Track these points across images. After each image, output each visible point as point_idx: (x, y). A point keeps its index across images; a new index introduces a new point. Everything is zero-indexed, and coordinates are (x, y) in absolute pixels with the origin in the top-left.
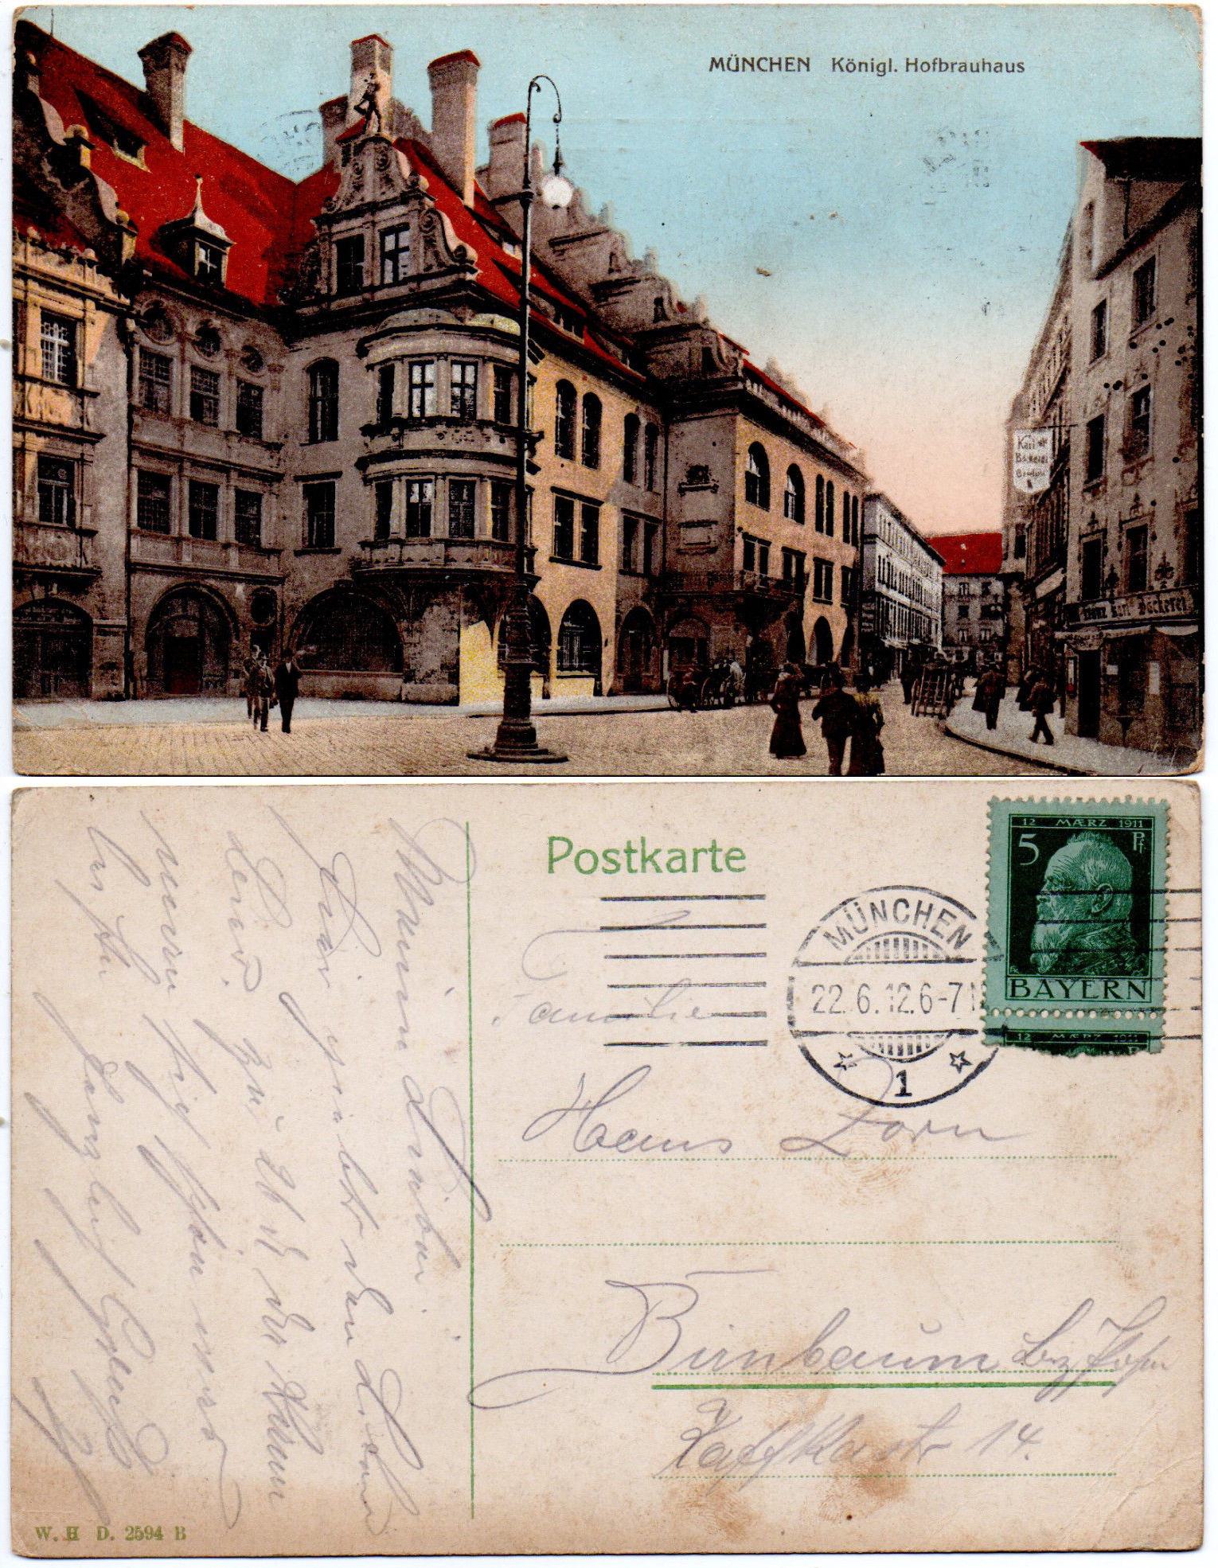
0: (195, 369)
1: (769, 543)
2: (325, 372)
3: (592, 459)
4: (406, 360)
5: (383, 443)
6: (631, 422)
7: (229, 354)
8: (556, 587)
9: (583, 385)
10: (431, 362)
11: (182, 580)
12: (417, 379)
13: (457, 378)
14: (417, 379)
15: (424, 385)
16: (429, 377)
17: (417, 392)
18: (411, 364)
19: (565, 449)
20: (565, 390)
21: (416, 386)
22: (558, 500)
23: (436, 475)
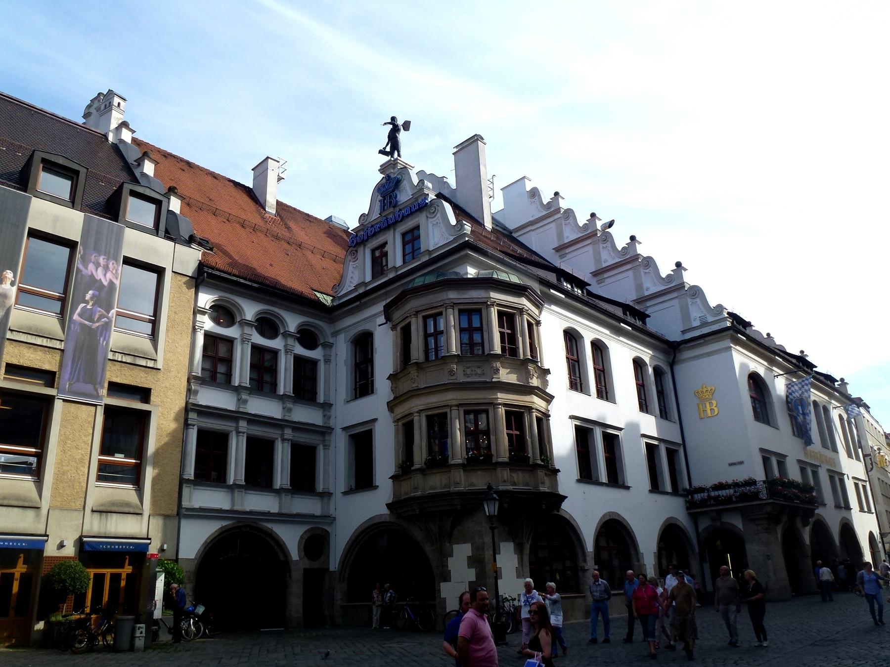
0: (256, 348)
1: (785, 456)
2: (363, 344)
3: (605, 392)
4: (420, 316)
5: (406, 386)
6: (638, 364)
7: (287, 335)
8: (585, 507)
9: (590, 331)
10: (440, 314)
11: (225, 523)
12: (431, 330)
13: (465, 325)
14: (431, 330)
15: (438, 333)
16: (442, 327)
17: (432, 341)
18: (425, 318)
19: (577, 383)
20: (572, 337)
21: (431, 335)
22: (578, 429)
23: (451, 406)
